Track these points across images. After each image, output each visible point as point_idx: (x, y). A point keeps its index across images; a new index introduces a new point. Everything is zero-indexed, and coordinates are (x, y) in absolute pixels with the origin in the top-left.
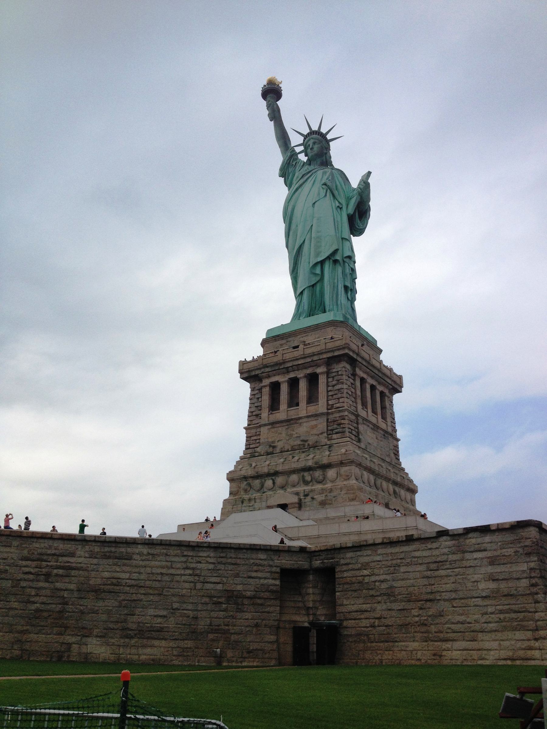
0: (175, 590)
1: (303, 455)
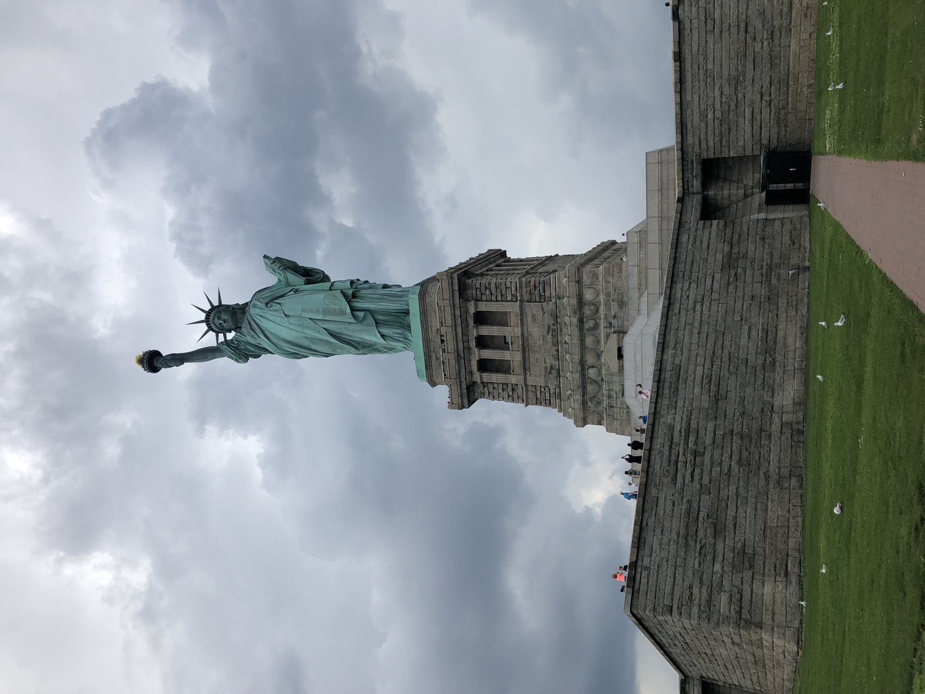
0: (719, 319)
1: (564, 330)
